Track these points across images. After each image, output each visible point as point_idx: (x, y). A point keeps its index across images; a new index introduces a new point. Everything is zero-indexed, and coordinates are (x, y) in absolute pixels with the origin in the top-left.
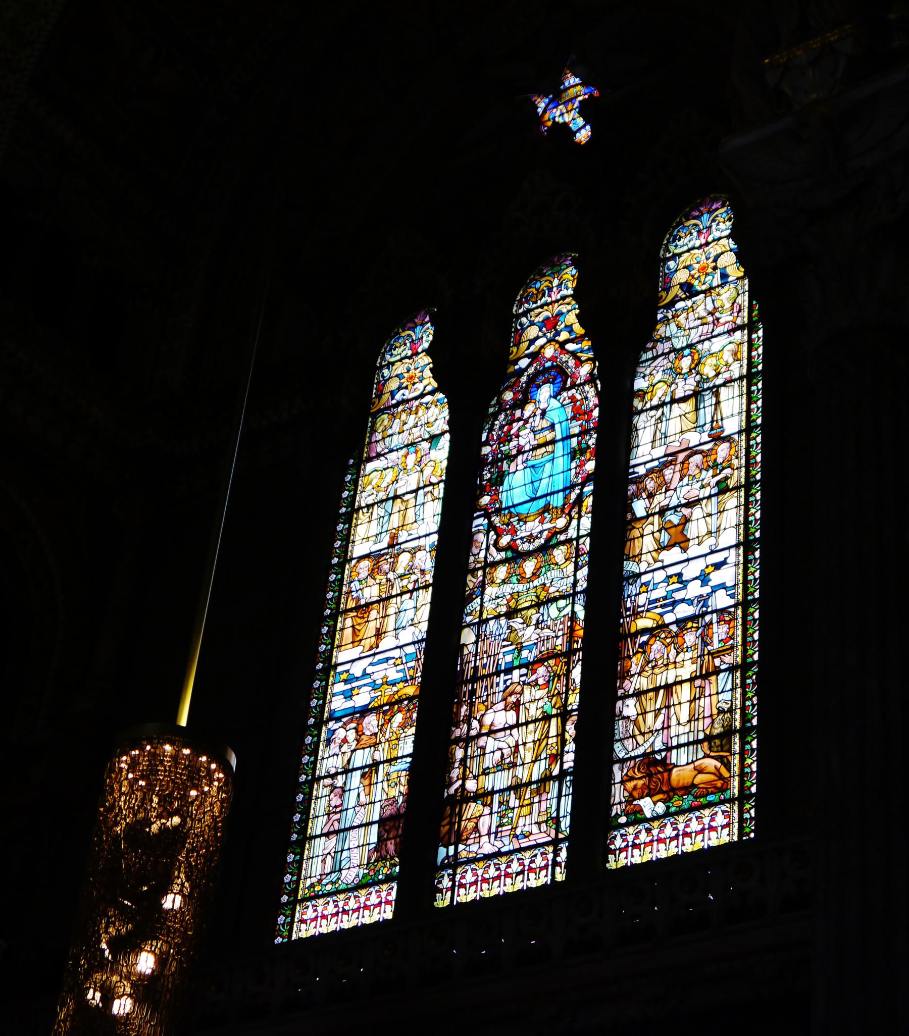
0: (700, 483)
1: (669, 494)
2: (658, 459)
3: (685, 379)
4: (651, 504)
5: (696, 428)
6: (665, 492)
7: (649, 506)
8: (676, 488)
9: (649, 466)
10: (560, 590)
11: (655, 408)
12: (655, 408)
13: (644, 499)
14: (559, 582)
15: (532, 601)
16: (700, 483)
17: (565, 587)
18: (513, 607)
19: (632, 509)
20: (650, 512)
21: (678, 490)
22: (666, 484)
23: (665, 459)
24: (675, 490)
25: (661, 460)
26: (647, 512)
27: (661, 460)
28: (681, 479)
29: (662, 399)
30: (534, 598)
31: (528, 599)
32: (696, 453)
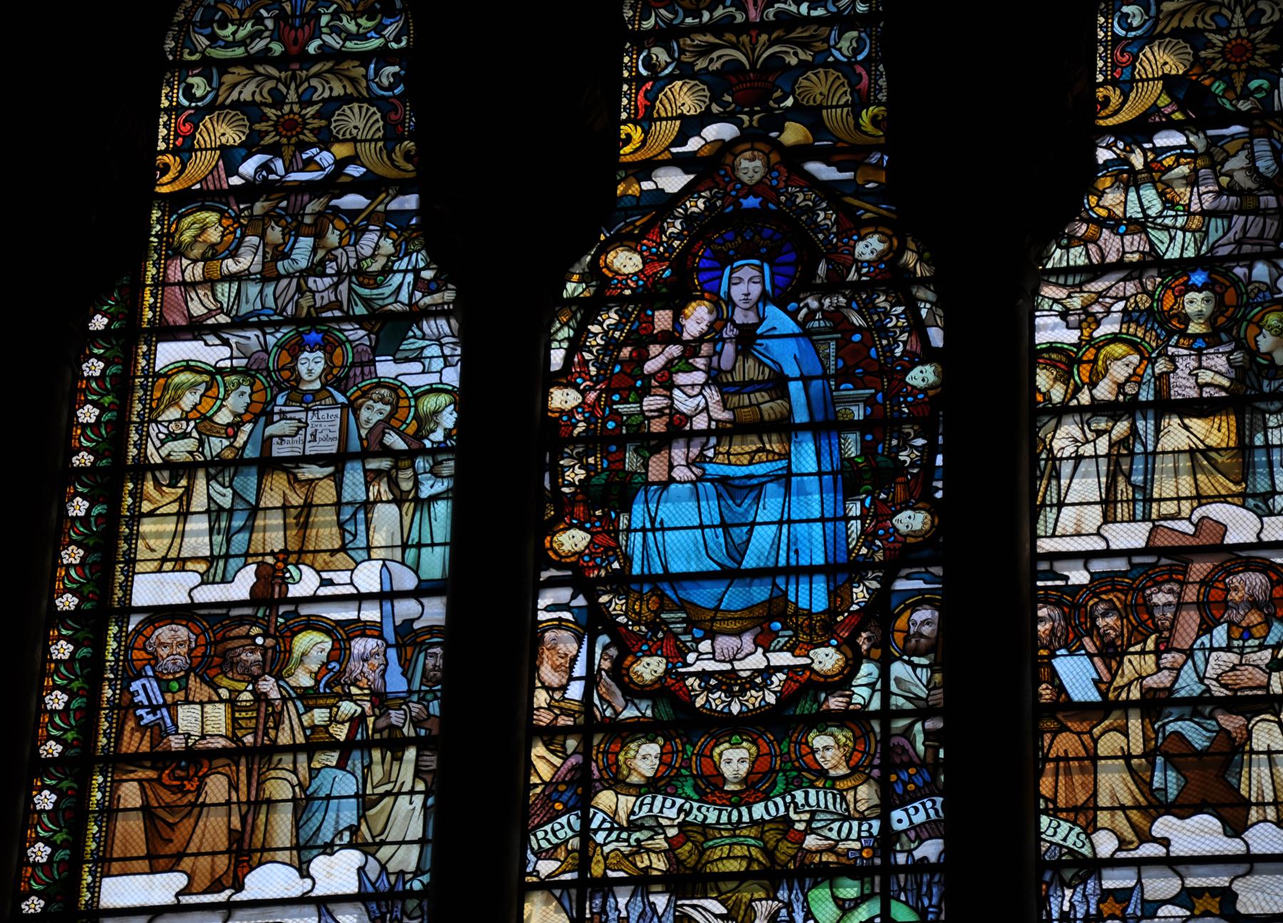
0: (1267, 654)
1: (1168, 659)
2: (1127, 553)
3: (1199, 353)
4: (1114, 677)
5: (1244, 495)
6: (1158, 653)
7: (1106, 677)
8: (1191, 649)
9: (1099, 566)
10: (841, 846)
11: (1111, 410)
12: (1111, 410)
13: (1090, 656)
14: (836, 826)
15: (750, 859)
16: (1267, 654)
17: (857, 845)
18: (691, 861)
19: (1054, 673)
20: (1111, 696)
21: (1199, 656)
22: (1157, 629)
23: (1150, 560)
24: (1189, 653)
25: (1136, 560)
26: (1103, 694)
27: (1136, 560)
28: (1206, 627)
29: (1130, 389)
30: (754, 852)
31: (738, 851)
32: (1250, 565)
